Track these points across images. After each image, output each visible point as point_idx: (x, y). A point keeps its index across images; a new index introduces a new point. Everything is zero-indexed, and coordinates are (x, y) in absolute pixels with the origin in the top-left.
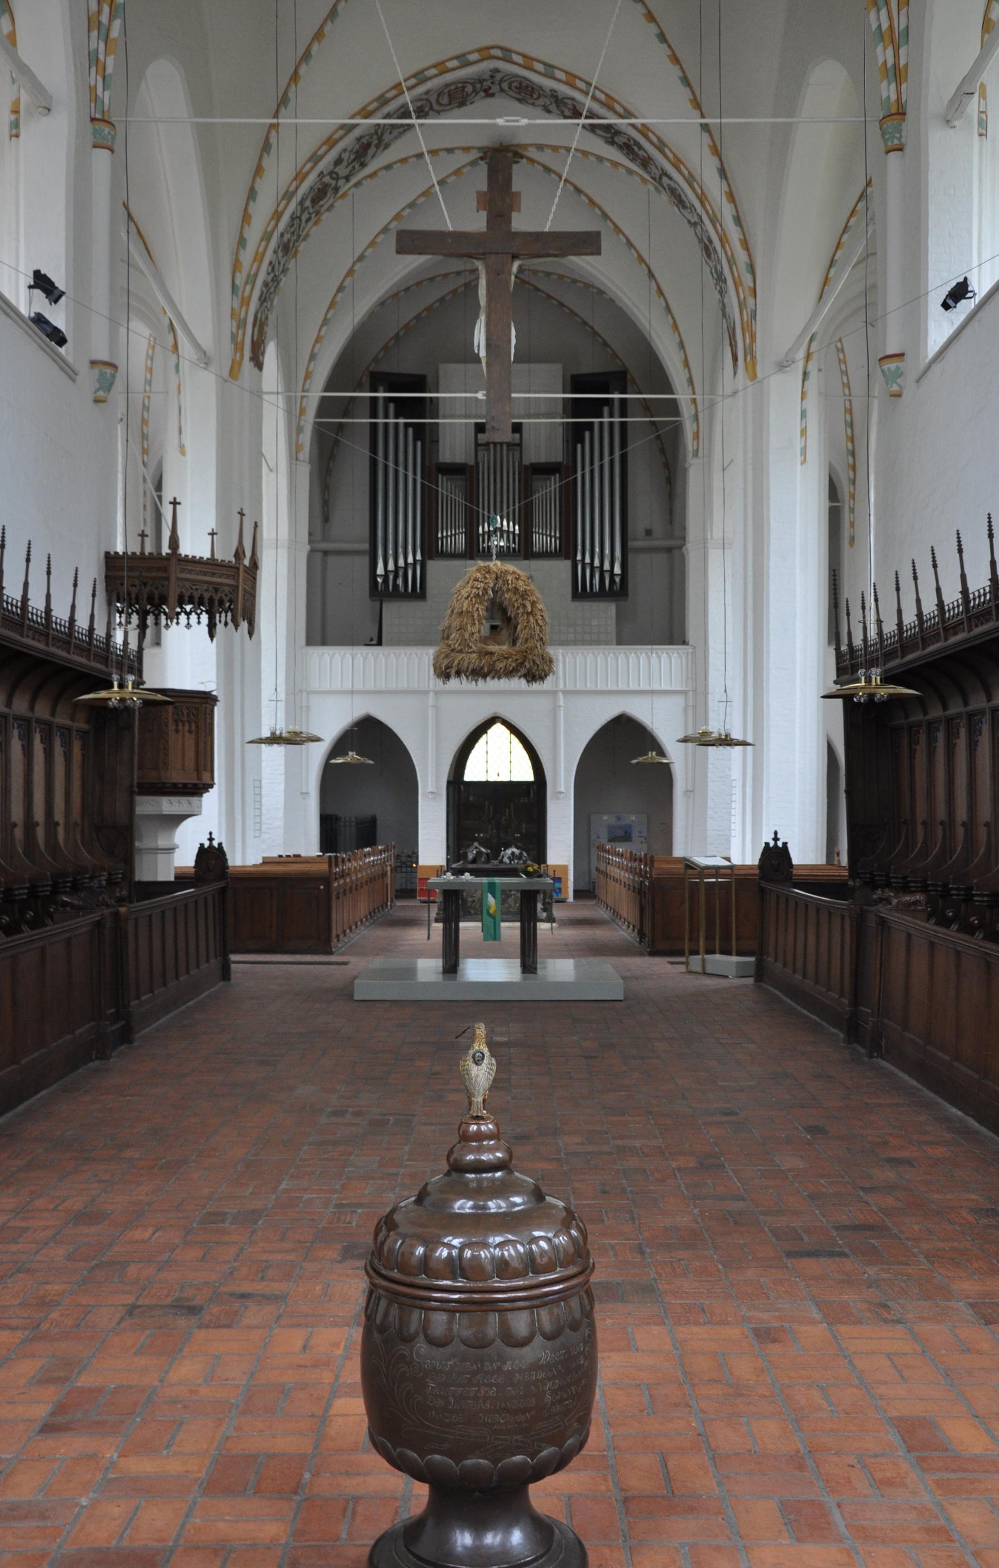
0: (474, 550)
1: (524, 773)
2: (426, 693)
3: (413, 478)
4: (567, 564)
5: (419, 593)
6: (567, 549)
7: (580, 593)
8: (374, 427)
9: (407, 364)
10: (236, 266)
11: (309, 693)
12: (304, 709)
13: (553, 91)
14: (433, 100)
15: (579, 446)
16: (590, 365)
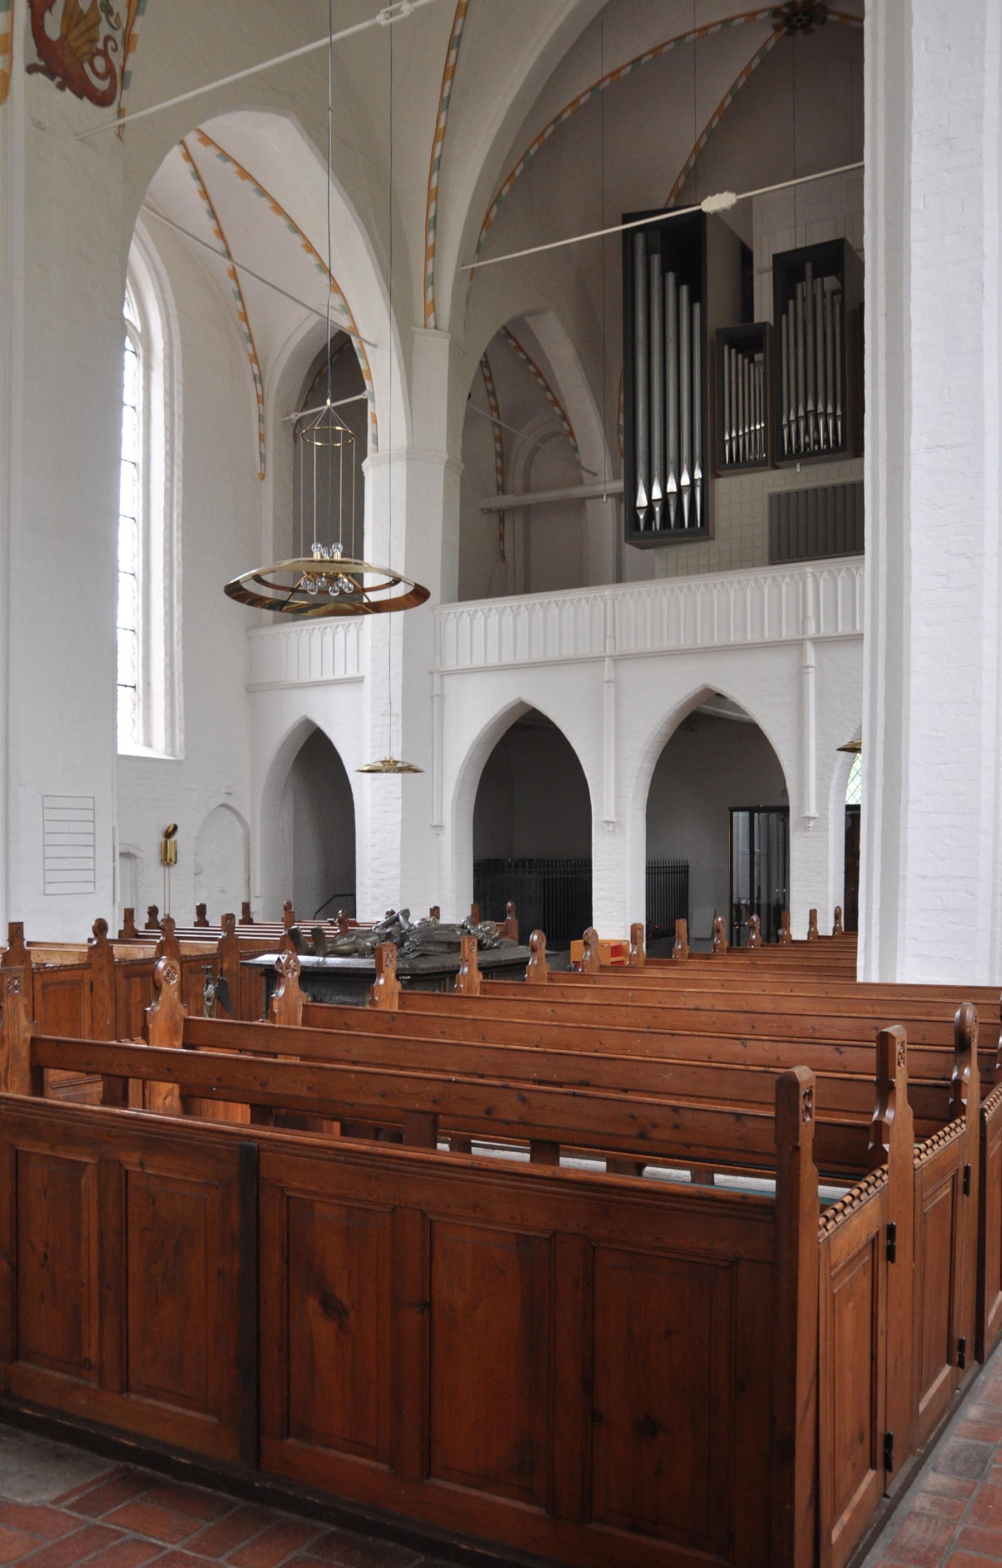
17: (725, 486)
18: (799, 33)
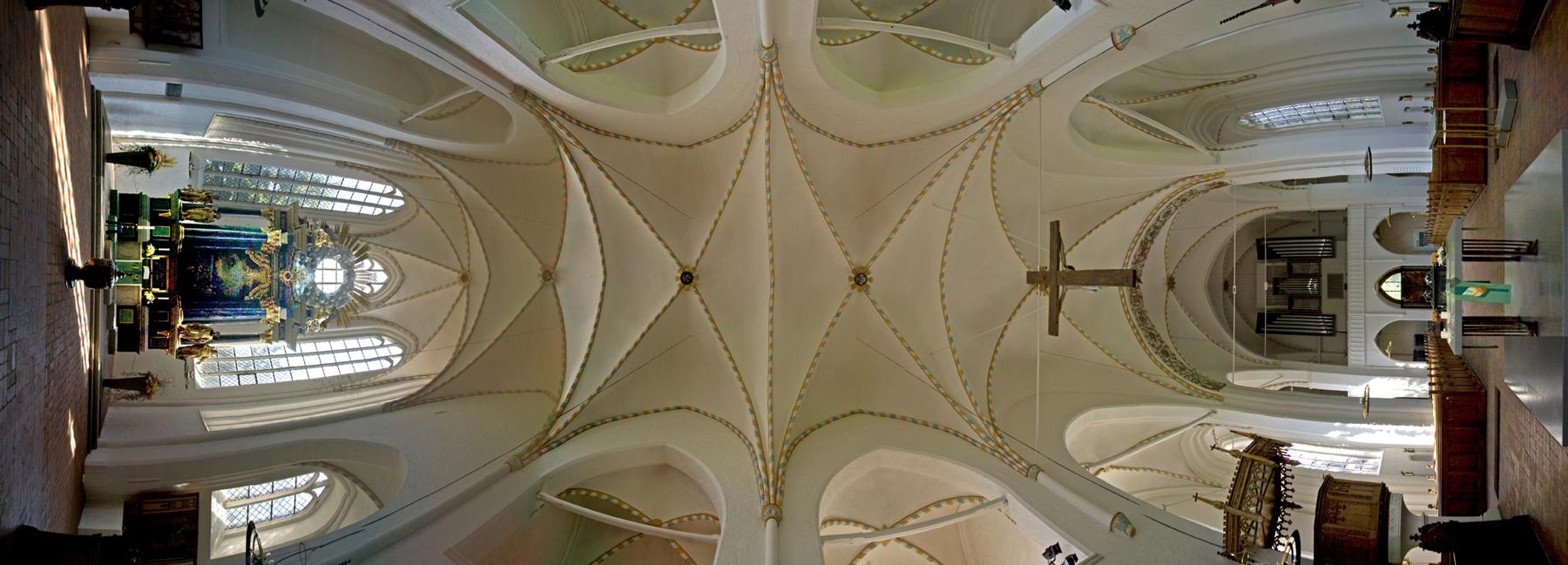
0: (1318, 297)
1: (1398, 277)
3: (1296, 319)
5: (1333, 317)
6: (1318, 260)
7: (1333, 255)
8: (1268, 332)
9: (1254, 319)
10: (1182, 392)
13: (1132, 263)
14: (1136, 308)
16: (1255, 253)
17: (1325, 310)
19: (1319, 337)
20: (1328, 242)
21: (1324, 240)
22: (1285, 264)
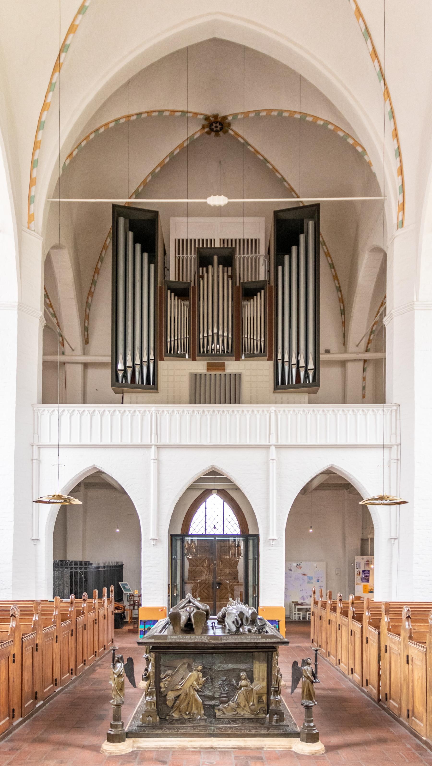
2: (148, 447)
4: (271, 363)
11: (40, 447)
12: (35, 461)
15: (280, 268)
18: (213, 134)
19: (109, 359)
20: (307, 376)
21: (311, 366)
22: (262, 277)
